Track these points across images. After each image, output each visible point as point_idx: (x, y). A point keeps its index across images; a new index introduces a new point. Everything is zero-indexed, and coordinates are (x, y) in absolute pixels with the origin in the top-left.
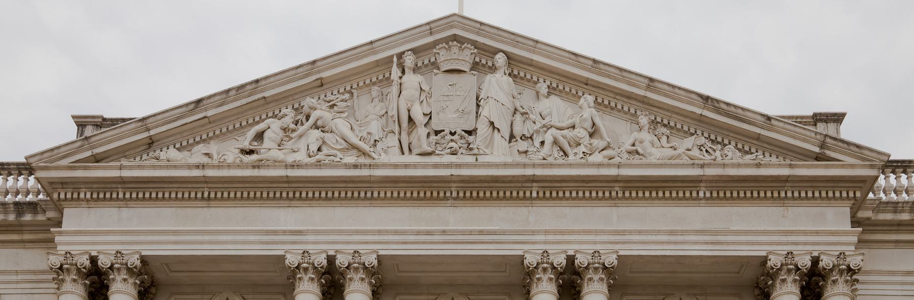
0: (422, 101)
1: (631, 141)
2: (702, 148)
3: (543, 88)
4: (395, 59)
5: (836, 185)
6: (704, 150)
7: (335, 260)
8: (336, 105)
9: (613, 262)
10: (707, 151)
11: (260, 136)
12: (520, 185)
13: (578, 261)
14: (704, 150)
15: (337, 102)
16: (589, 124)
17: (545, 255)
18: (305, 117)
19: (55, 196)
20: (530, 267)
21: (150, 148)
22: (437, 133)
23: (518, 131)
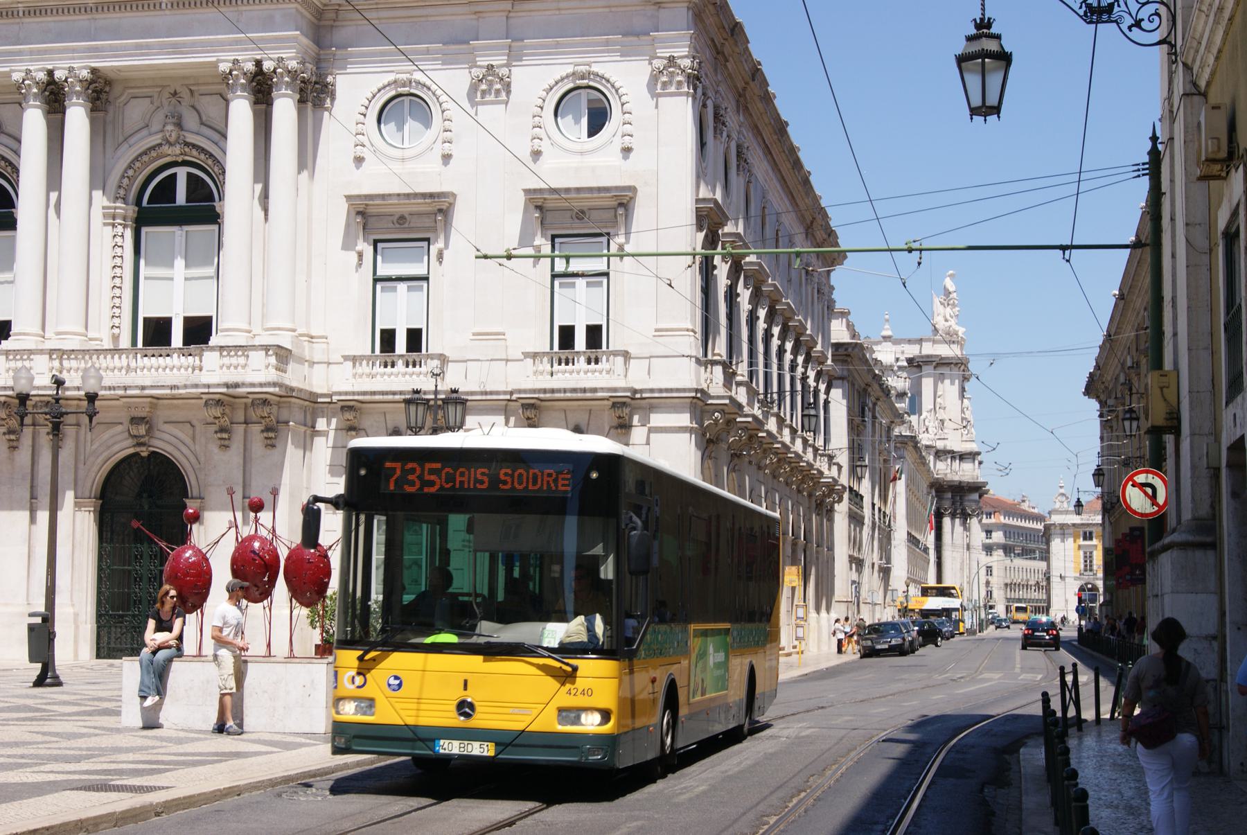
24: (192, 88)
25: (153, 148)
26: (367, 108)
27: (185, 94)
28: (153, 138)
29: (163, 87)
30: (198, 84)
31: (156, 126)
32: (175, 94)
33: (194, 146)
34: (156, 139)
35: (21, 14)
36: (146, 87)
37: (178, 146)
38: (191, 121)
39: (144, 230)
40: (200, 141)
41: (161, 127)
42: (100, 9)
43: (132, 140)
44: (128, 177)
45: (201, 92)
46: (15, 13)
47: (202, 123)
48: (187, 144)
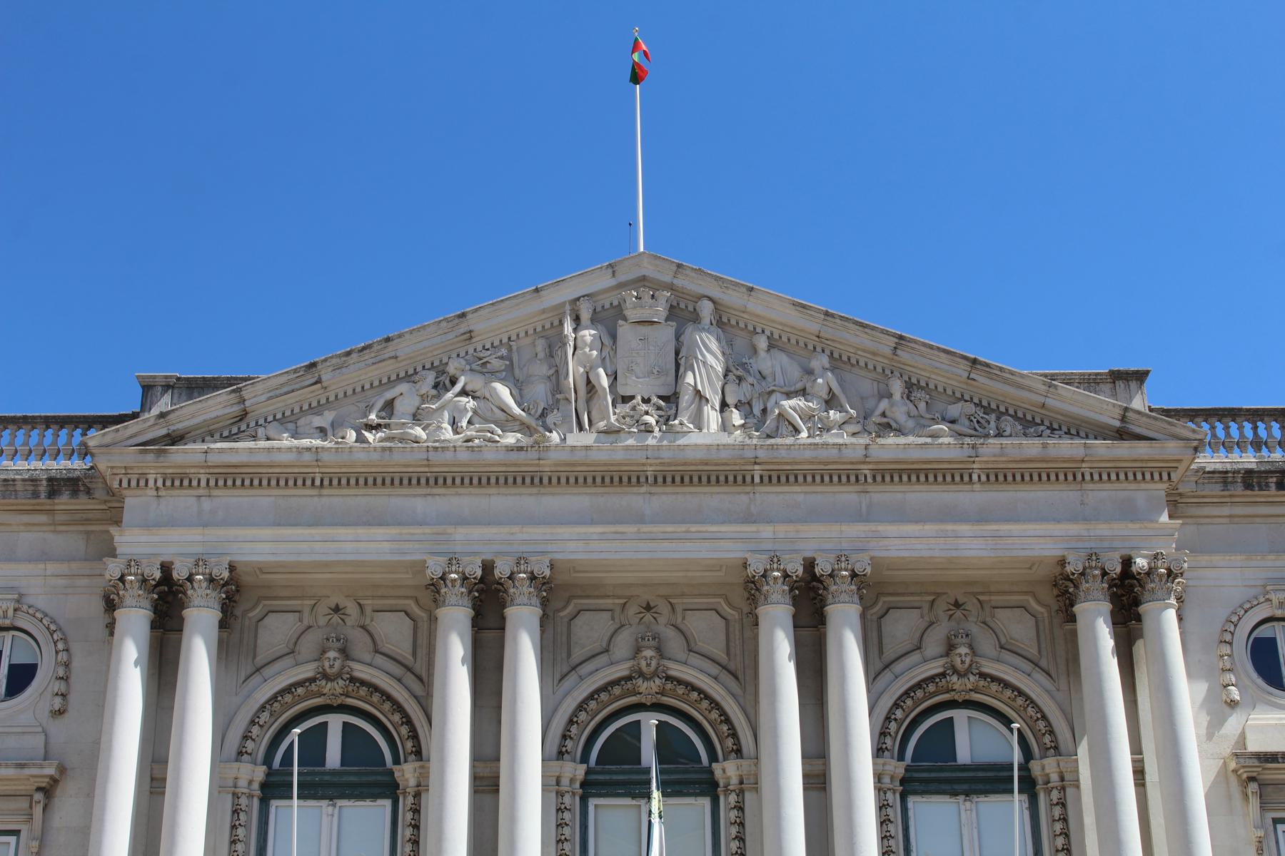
0: (604, 358)
1: (878, 412)
2: (972, 418)
3: (762, 343)
4: (568, 307)
5: (1144, 465)
6: (975, 420)
7: (493, 568)
8: (490, 363)
9: (865, 569)
10: (978, 422)
11: (389, 406)
12: (737, 468)
13: (820, 568)
14: (975, 420)
15: (491, 359)
16: (826, 390)
17: (775, 560)
18: (448, 378)
19: (116, 485)
20: (755, 576)
21: (241, 420)
22: (626, 399)
23: (730, 400)
24: (981, 598)
25: (931, 679)
26: (1232, 634)
27: (972, 605)
28: (932, 665)
29: (938, 595)
30: (990, 593)
31: (933, 644)
32: (957, 605)
33: (994, 679)
34: (935, 668)
35: (757, 479)
36: (912, 594)
37: (972, 678)
38: (986, 644)
39: (912, 801)
40: (1005, 673)
41: (940, 649)
42: (879, 478)
43: (898, 667)
44: (895, 720)
45: (993, 604)
46: (748, 479)
47: (1002, 647)
48: (983, 676)
